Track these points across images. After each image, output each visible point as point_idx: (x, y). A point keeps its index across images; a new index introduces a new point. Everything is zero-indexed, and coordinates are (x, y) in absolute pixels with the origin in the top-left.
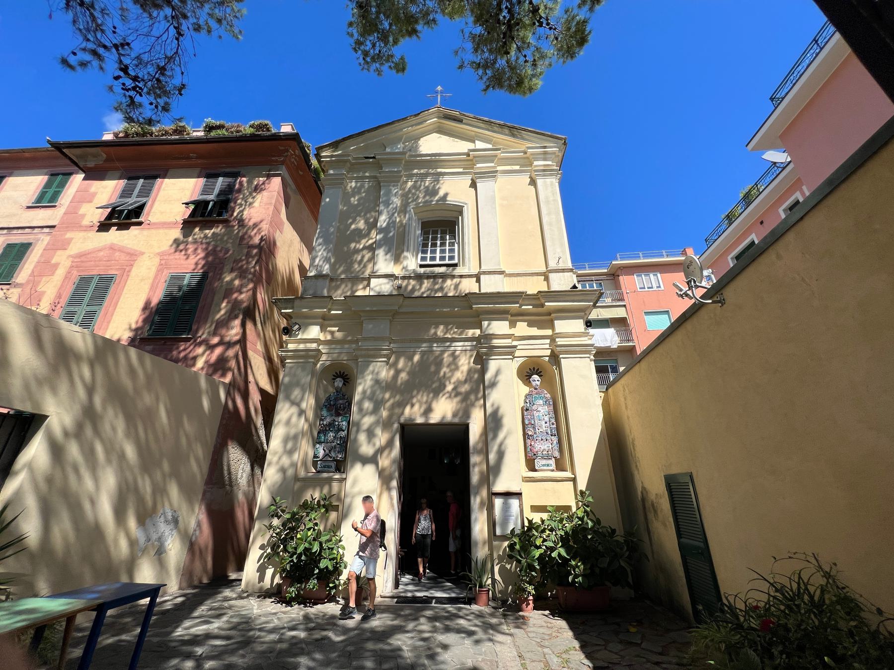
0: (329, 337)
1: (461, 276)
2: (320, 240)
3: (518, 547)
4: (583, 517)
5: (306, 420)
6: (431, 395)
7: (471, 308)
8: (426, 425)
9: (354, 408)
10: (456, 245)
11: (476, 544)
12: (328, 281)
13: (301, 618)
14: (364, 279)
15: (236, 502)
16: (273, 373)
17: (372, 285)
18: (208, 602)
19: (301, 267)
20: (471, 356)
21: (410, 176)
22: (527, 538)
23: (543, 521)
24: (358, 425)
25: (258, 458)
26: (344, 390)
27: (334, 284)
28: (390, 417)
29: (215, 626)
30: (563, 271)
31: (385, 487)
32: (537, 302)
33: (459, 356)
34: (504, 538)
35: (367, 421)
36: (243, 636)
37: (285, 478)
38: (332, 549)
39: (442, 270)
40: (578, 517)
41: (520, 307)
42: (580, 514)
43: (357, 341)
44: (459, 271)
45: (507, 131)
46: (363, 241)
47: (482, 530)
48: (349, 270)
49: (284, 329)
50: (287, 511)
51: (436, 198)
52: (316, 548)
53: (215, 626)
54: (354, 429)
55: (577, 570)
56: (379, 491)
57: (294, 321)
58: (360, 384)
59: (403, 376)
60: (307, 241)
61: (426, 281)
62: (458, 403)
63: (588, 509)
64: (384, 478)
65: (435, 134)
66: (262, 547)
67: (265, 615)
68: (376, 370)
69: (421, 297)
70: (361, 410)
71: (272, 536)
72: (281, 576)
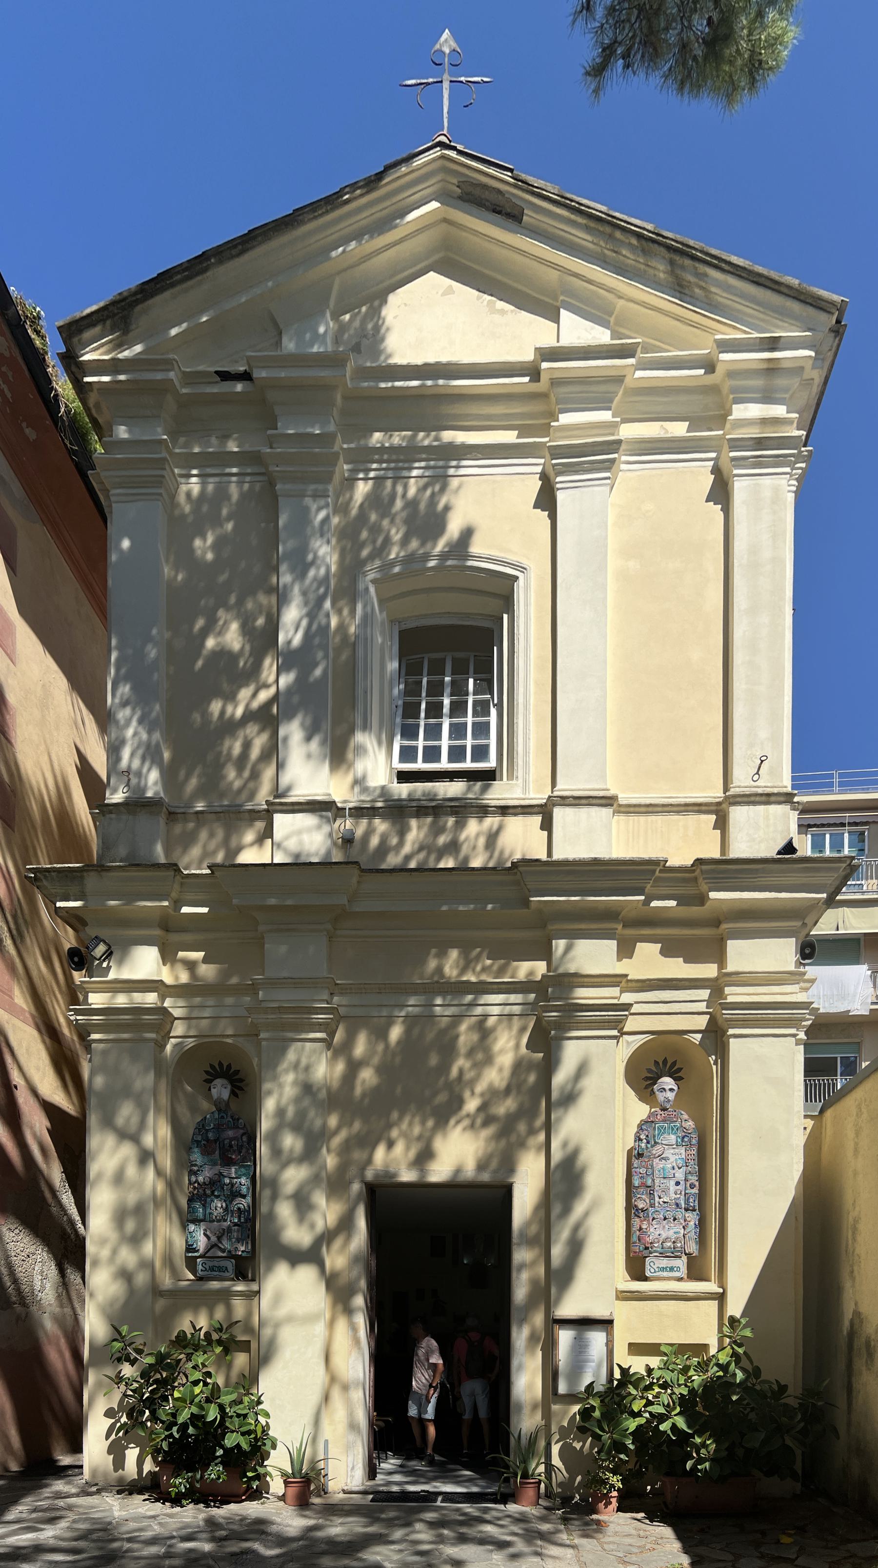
0: (184, 977)
1: (504, 810)
2: (125, 689)
3: (597, 1414)
4: (729, 1364)
5: (159, 1173)
6: (430, 1123)
7: (526, 903)
8: (422, 1186)
9: (263, 1149)
10: (493, 711)
11: (519, 1407)
12: (162, 821)
13: (201, 1523)
14: (254, 815)
15: (41, 1335)
16: (64, 1063)
17: (278, 834)
18: (28, 1499)
19: (85, 770)
20: (523, 1030)
21: (362, 458)
22: (617, 1399)
23: (649, 1371)
24: (274, 1184)
25: (69, 1252)
26: (233, 1106)
27: (178, 829)
28: (342, 1168)
29: (48, 1534)
30: (767, 798)
31: (340, 1307)
32: (690, 890)
33: (493, 1030)
34: (571, 1398)
35: (294, 1176)
36: (101, 1549)
37: (131, 1291)
38: (245, 1416)
39: (454, 789)
40: (718, 1365)
41: (647, 902)
42: (723, 1358)
43: (253, 989)
44: (500, 793)
45: (660, 269)
46: (244, 694)
47: (530, 1386)
48: (212, 784)
49: (73, 953)
50: (146, 1351)
51: (440, 545)
52: (212, 1414)
53: (48, 1534)
54: (267, 1193)
55: (703, 1451)
56: (328, 1316)
57: (91, 932)
58: (269, 1093)
59: (367, 1076)
60: (86, 686)
61: (414, 823)
62: (488, 1140)
63: (740, 1351)
64: (338, 1291)
65: (432, 276)
66: (109, 1413)
67: (135, 1519)
68: (304, 1061)
69: (401, 870)
70: (276, 1151)
71: (125, 1395)
72: (154, 1459)
